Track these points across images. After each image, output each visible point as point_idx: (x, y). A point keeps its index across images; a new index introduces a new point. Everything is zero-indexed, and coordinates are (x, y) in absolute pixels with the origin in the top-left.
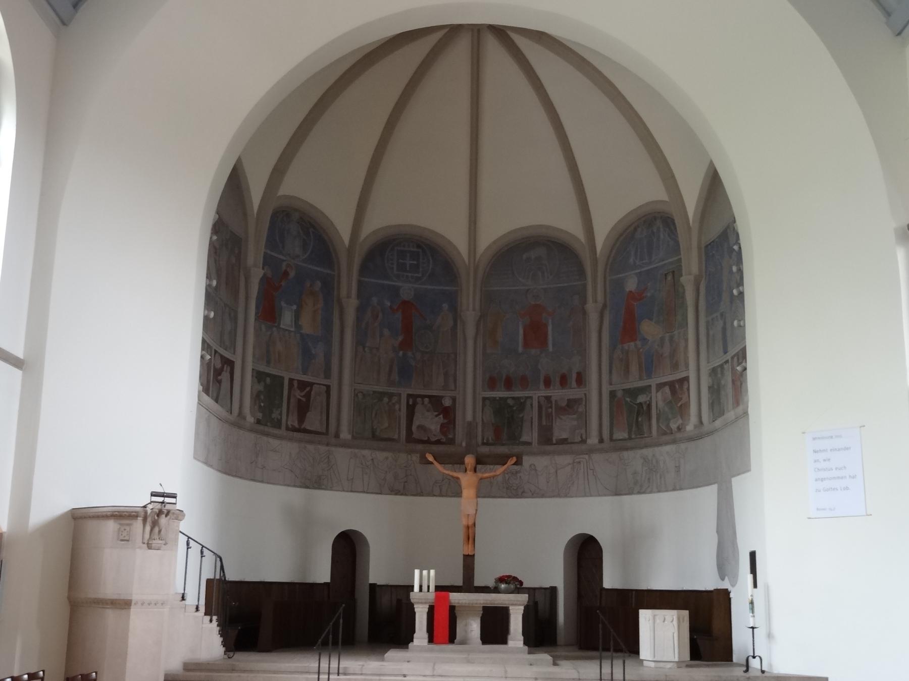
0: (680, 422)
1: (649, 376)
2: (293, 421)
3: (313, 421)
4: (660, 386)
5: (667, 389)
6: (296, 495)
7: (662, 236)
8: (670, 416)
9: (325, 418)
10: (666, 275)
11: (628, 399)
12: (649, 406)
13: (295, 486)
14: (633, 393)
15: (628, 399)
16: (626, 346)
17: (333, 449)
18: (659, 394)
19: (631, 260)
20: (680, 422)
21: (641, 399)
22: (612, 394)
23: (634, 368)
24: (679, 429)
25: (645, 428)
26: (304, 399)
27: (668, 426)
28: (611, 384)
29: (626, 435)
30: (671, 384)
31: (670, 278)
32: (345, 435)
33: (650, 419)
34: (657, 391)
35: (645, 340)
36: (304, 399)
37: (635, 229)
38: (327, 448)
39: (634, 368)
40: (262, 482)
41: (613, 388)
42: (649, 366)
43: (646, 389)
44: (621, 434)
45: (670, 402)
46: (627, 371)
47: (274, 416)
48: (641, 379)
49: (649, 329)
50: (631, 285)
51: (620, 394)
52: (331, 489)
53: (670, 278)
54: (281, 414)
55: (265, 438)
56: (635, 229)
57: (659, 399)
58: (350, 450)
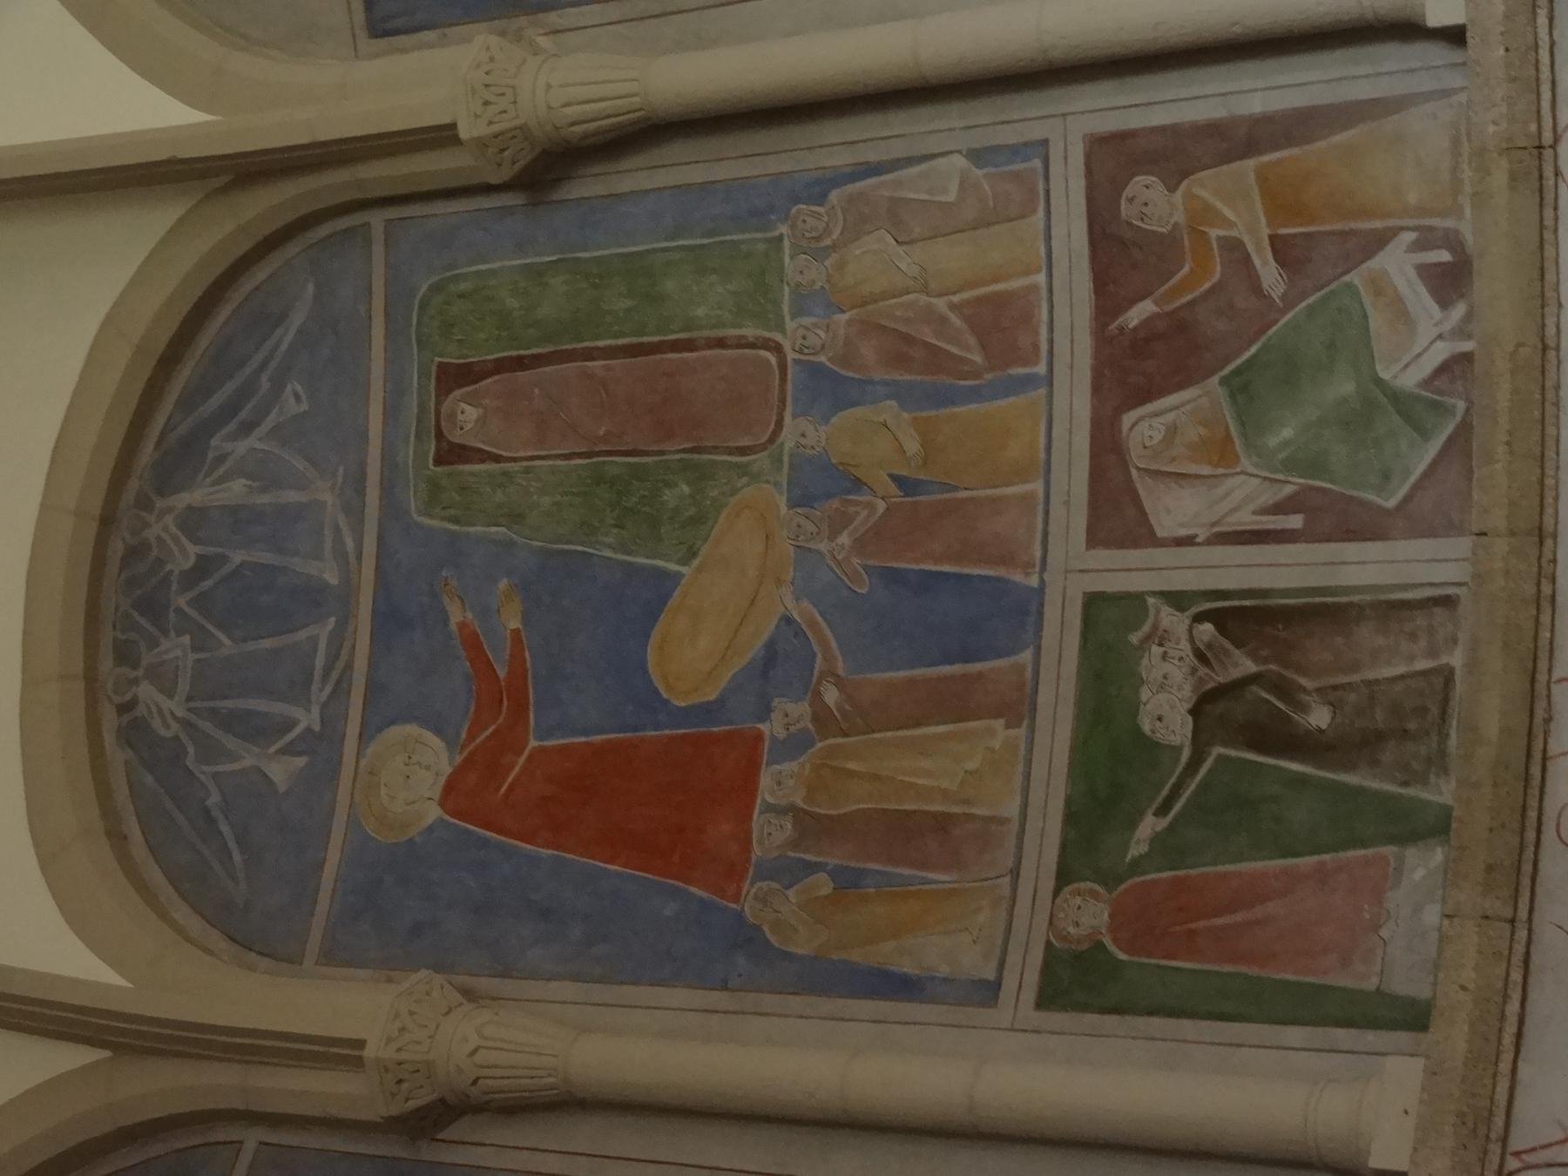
0: (1398, 265)
1: (1020, 613)
4: (1116, 514)
5: (1144, 427)
7: (237, 490)
8: (1344, 387)
10: (452, 453)
11: (1149, 825)
12: (1240, 618)
14: (1112, 768)
15: (1149, 825)
16: (769, 835)
18: (1174, 510)
19: (281, 771)
20: (1398, 265)
21: (1165, 705)
22: (1077, 983)
23: (936, 766)
24: (1449, 281)
25: (1393, 662)
27: (1413, 411)
28: (987, 992)
29: (1422, 865)
30: (1134, 369)
31: (467, 416)
33: (1325, 614)
34: (1140, 534)
35: (780, 662)
37: (135, 732)
39: (936, 766)
41: (1024, 974)
42: (941, 616)
43: (1107, 617)
44: (1415, 914)
45: (1240, 388)
46: (927, 835)
48: (1018, 706)
49: (724, 608)
50: (408, 776)
51: (1089, 915)
53: (467, 416)
56: (135, 732)
57: (1211, 523)
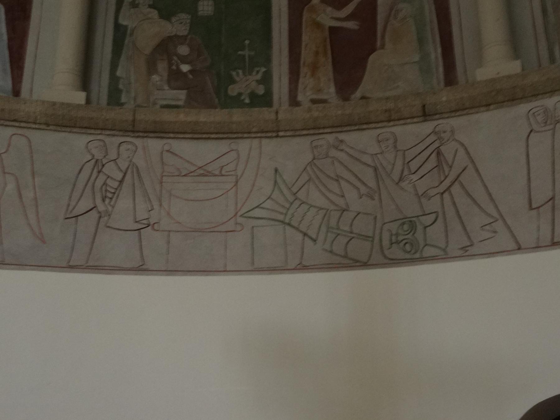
2: (320, 84)
3: (396, 67)
6: (314, 301)
9: (435, 52)
13: (302, 268)
17: (446, 124)
26: (352, 25)
32: (495, 63)
36: (352, 25)
38: (427, 127)
40: (141, 269)
47: (233, 90)
52: (466, 252)
54: (266, 80)
55: (155, 145)
58: (523, 108)
